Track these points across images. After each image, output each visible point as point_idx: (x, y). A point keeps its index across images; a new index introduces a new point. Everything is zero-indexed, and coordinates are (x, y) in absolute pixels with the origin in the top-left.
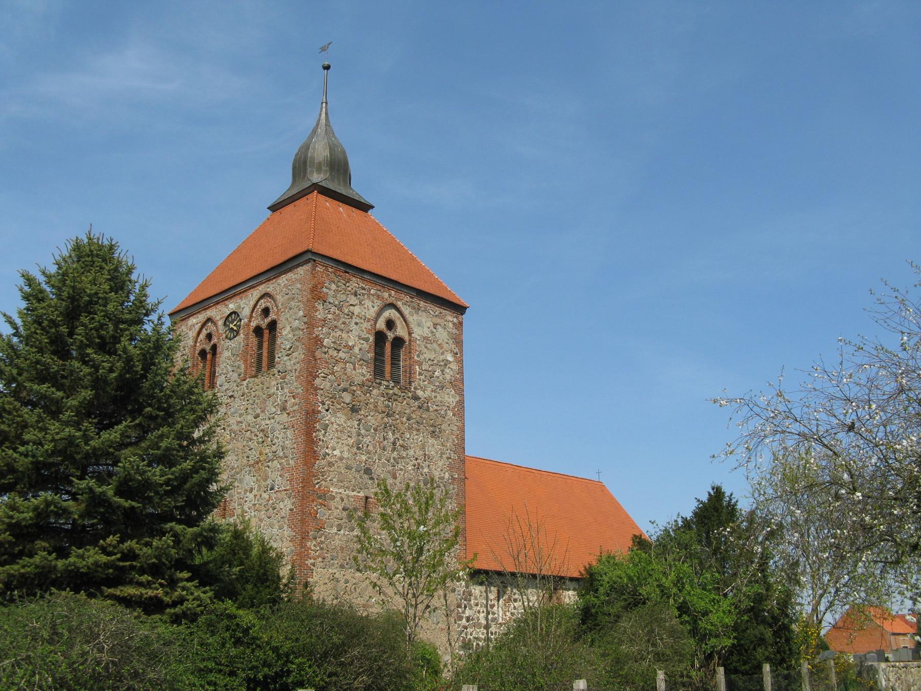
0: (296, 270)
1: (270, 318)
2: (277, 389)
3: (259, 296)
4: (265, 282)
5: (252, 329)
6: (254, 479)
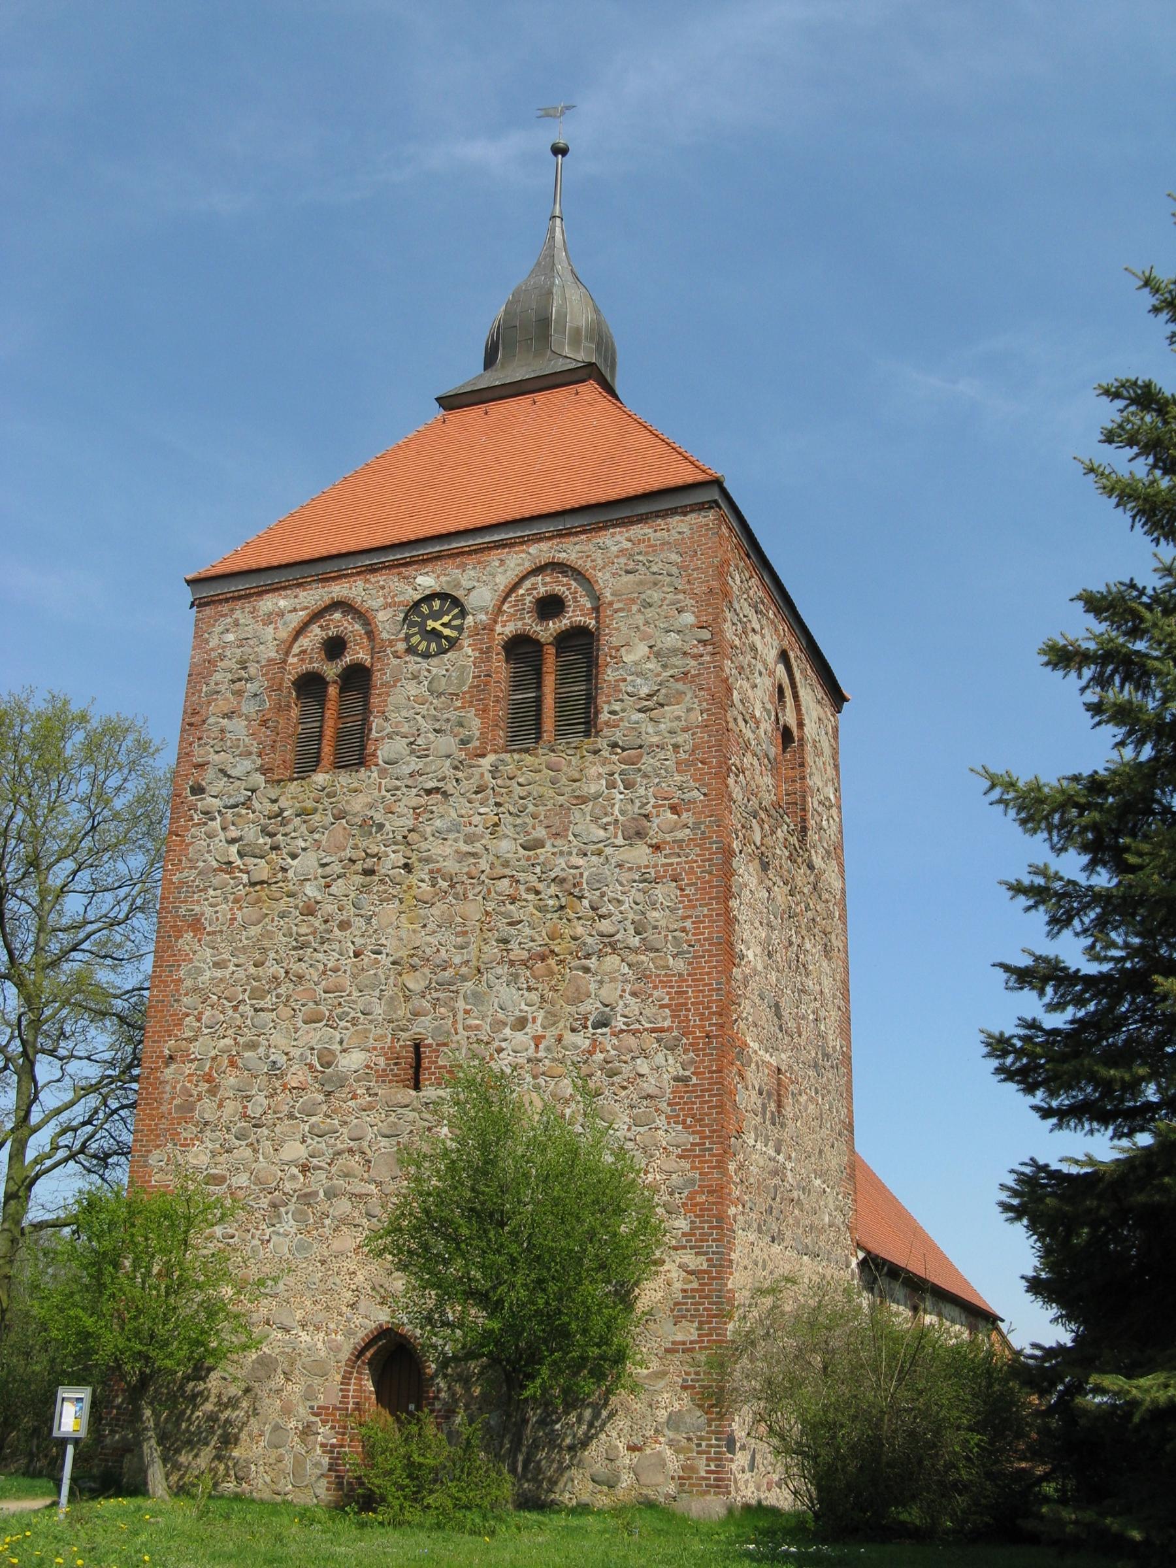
0: (659, 521)
1: (565, 621)
2: (611, 785)
3: (528, 566)
4: (550, 538)
5: (498, 640)
6: (534, 996)
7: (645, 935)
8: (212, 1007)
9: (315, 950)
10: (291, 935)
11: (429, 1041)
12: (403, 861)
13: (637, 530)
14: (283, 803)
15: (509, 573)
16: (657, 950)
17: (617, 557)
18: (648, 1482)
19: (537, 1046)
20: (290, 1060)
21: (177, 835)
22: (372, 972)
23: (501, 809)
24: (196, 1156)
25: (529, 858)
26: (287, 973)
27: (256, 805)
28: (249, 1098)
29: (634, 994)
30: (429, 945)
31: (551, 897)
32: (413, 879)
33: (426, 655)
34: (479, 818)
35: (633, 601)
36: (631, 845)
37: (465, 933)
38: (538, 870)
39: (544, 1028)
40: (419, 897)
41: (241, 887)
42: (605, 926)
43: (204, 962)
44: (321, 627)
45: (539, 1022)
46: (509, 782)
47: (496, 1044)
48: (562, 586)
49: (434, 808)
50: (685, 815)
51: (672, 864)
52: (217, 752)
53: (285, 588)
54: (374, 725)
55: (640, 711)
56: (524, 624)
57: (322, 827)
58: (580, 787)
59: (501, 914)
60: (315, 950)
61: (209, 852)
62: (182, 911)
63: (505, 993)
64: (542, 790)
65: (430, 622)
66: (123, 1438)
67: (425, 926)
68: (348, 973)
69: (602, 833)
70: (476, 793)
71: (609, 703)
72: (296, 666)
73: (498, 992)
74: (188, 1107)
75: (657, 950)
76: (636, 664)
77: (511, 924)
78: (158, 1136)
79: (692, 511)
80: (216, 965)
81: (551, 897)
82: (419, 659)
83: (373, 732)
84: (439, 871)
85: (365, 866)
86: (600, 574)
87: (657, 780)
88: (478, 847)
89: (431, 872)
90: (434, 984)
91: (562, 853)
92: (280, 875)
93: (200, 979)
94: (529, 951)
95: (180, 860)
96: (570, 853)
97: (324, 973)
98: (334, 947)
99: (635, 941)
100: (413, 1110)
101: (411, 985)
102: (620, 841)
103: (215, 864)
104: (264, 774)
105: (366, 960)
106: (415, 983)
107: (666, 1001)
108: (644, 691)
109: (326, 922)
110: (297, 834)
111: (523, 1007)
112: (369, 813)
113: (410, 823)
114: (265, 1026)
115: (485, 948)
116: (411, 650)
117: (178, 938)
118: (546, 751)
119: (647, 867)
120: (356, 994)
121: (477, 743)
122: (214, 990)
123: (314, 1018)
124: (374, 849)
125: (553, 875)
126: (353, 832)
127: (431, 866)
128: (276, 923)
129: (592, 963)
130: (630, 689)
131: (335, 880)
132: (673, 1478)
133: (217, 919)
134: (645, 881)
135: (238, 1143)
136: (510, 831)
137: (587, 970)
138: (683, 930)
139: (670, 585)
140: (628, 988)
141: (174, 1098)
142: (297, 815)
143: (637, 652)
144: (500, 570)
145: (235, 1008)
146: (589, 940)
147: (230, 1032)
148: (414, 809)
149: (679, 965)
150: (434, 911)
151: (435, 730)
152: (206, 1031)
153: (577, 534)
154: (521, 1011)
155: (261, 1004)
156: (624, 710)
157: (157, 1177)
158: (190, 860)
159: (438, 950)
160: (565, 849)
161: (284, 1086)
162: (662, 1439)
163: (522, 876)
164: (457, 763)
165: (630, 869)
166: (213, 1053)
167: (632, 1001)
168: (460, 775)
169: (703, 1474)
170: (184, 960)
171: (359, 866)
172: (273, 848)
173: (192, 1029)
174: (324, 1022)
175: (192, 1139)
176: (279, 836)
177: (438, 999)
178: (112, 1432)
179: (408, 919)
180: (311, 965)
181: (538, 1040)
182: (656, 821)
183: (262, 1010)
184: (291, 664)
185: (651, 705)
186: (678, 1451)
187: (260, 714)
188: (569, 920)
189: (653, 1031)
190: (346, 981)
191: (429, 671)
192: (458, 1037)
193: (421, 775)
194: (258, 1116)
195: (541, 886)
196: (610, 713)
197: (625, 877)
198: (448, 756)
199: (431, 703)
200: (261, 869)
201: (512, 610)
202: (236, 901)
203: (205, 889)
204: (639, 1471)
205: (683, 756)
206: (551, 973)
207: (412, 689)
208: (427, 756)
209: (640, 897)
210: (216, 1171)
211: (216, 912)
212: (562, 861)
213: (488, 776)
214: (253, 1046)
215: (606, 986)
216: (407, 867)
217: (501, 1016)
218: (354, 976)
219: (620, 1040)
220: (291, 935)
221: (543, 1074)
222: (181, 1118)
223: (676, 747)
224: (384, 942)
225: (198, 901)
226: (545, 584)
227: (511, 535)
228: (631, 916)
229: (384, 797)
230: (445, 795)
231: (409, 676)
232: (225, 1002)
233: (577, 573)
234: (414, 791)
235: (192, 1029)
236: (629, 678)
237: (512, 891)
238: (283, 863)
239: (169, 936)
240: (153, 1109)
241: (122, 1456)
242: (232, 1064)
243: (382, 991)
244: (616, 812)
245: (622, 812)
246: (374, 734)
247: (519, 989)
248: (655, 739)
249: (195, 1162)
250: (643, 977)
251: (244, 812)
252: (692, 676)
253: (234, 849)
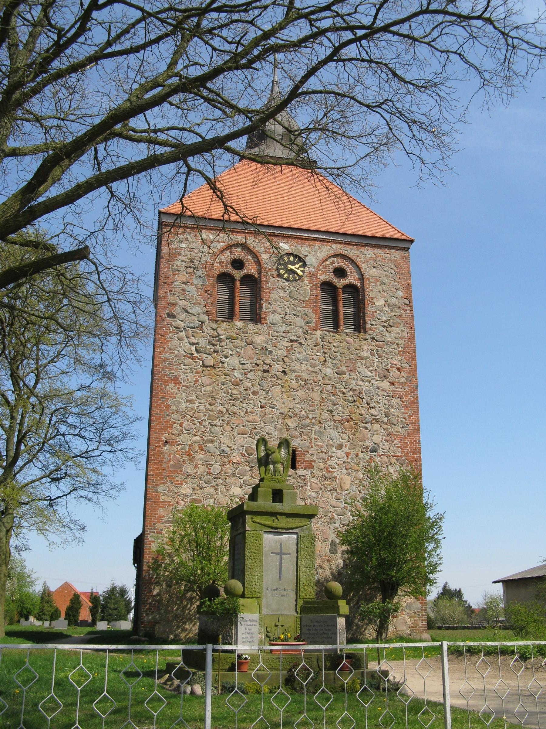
0: (386, 250)
2: (373, 355)
3: (331, 253)
4: (340, 243)
5: (319, 282)
6: (345, 436)
7: (389, 418)
8: (188, 420)
9: (241, 402)
10: (228, 393)
11: (300, 449)
12: (282, 370)
13: (377, 251)
14: (220, 331)
15: (323, 253)
16: (395, 425)
17: (370, 260)
18: (400, 629)
19: (347, 457)
20: (232, 450)
21: (161, 335)
22: (270, 416)
23: (326, 355)
24: (185, 489)
25: (340, 378)
26: (227, 410)
27: (205, 329)
28: (211, 465)
29: (386, 441)
30: (297, 408)
31: (350, 396)
32: (287, 378)
33: (287, 280)
34: (316, 357)
35: (378, 280)
36: (382, 381)
37: (313, 406)
38: (344, 384)
39: (350, 449)
40: (291, 386)
41: (199, 366)
42: (373, 411)
43: (182, 399)
44: (230, 252)
45: (348, 447)
46: (329, 345)
47: (330, 454)
48: (346, 266)
49: (296, 349)
50: (403, 373)
51: (399, 391)
52: (181, 300)
53: (212, 229)
54: (264, 305)
55: (383, 326)
56: (330, 277)
57: (241, 346)
58: (360, 353)
59: (329, 400)
60: (241, 402)
61: (180, 347)
62: (167, 372)
63: (334, 434)
64: (344, 351)
65: (290, 266)
66: (154, 618)
67: (294, 399)
68: (259, 415)
69: (370, 373)
70: (315, 346)
71: (370, 320)
72: (218, 269)
73: (329, 432)
74: (178, 467)
75: (395, 425)
76: (380, 307)
77: (333, 405)
78: (162, 478)
79: (400, 250)
80: (188, 401)
81: (350, 396)
82: (284, 281)
83: (264, 308)
84: (299, 376)
85: (264, 368)
86: (363, 265)
87: (391, 357)
88: (317, 369)
89: (296, 376)
90: (300, 425)
91: (354, 379)
92: (220, 364)
93: (180, 407)
94: (342, 417)
95: (164, 348)
96: (357, 379)
97: (247, 413)
98: (251, 402)
99: (386, 420)
100: (294, 478)
101: (290, 424)
102: (377, 378)
103: (185, 354)
104: (208, 316)
105: (267, 410)
106: (292, 423)
107: (399, 445)
108: (384, 319)
109: (246, 390)
110: (228, 347)
111: (340, 440)
112: (265, 345)
113: (285, 353)
114: (217, 433)
115: (323, 413)
116: (279, 275)
117: (166, 386)
118: (344, 335)
119: (389, 391)
120: (263, 425)
121: (314, 325)
122: (188, 413)
123: (243, 433)
124: (268, 362)
125: (351, 387)
126: (257, 352)
127: (296, 374)
128: (220, 387)
129: (369, 426)
130: (378, 317)
131: (249, 372)
132: (409, 627)
133: (188, 380)
134: (388, 396)
135: (206, 485)
136: (330, 365)
137: (366, 428)
138: (404, 418)
139: (392, 278)
140: (384, 438)
141: (170, 461)
142: (227, 339)
143: (380, 302)
144: (319, 251)
145: (200, 423)
146: (367, 416)
147: (198, 434)
148: (286, 347)
149: (403, 431)
150: (298, 393)
151: (294, 314)
152: (185, 432)
153: (352, 245)
154: (340, 441)
155: (215, 423)
156: (376, 325)
157: (163, 498)
158: (170, 349)
159: (301, 411)
160: (355, 377)
161: (229, 461)
162: (404, 613)
163: (337, 386)
164: (305, 331)
165: (383, 390)
166: (190, 442)
167: (386, 443)
168: (307, 337)
169: (421, 626)
170: (171, 397)
171: (261, 368)
172: (215, 351)
173: (177, 430)
174: (248, 435)
175: (181, 481)
176: (218, 346)
177: (303, 432)
178: (147, 615)
179: (286, 395)
180: (240, 409)
181: (348, 455)
182: (392, 373)
183: (215, 425)
184: (216, 266)
185: (388, 326)
186: (410, 618)
187: (203, 287)
188: (358, 407)
189: (395, 456)
190: (257, 418)
191: (289, 287)
192: (312, 449)
193: (288, 333)
194: (216, 473)
195: (345, 391)
196: (371, 324)
197: (380, 393)
198: (301, 327)
199: (291, 302)
200: (210, 361)
201: (324, 270)
202: (197, 373)
203: (180, 364)
204: (396, 625)
205: (401, 349)
206: (352, 428)
207: (281, 293)
208: (291, 325)
209: (386, 402)
210: (196, 497)
211: (187, 376)
212: (354, 382)
213: (319, 339)
214: (212, 442)
215: (375, 436)
216: (284, 372)
217: (331, 442)
218: (262, 417)
219: (381, 458)
220: (228, 393)
221: (351, 468)
222: (175, 471)
223: (398, 344)
224: (276, 403)
225: (176, 370)
226: (338, 262)
227: (324, 237)
228: (383, 409)
229: (272, 339)
230: (301, 344)
231: (280, 287)
232: (195, 419)
233: (353, 262)
234: (286, 339)
235: (177, 430)
236: (378, 312)
237: (333, 391)
238: (222, 360)
239: (161, 384)
240: (158, 465)
241: (154, 625)
242: (201, 449)
243: (276, 425)
244: (375, 366)
245: (378, 367)
246: (264, 309)
247: (338, 432)
248: (390, 340)
249: (184, 492)
250: (390, 434)
251: (199, 331)
252: (404, 318)
253: (193, 348)
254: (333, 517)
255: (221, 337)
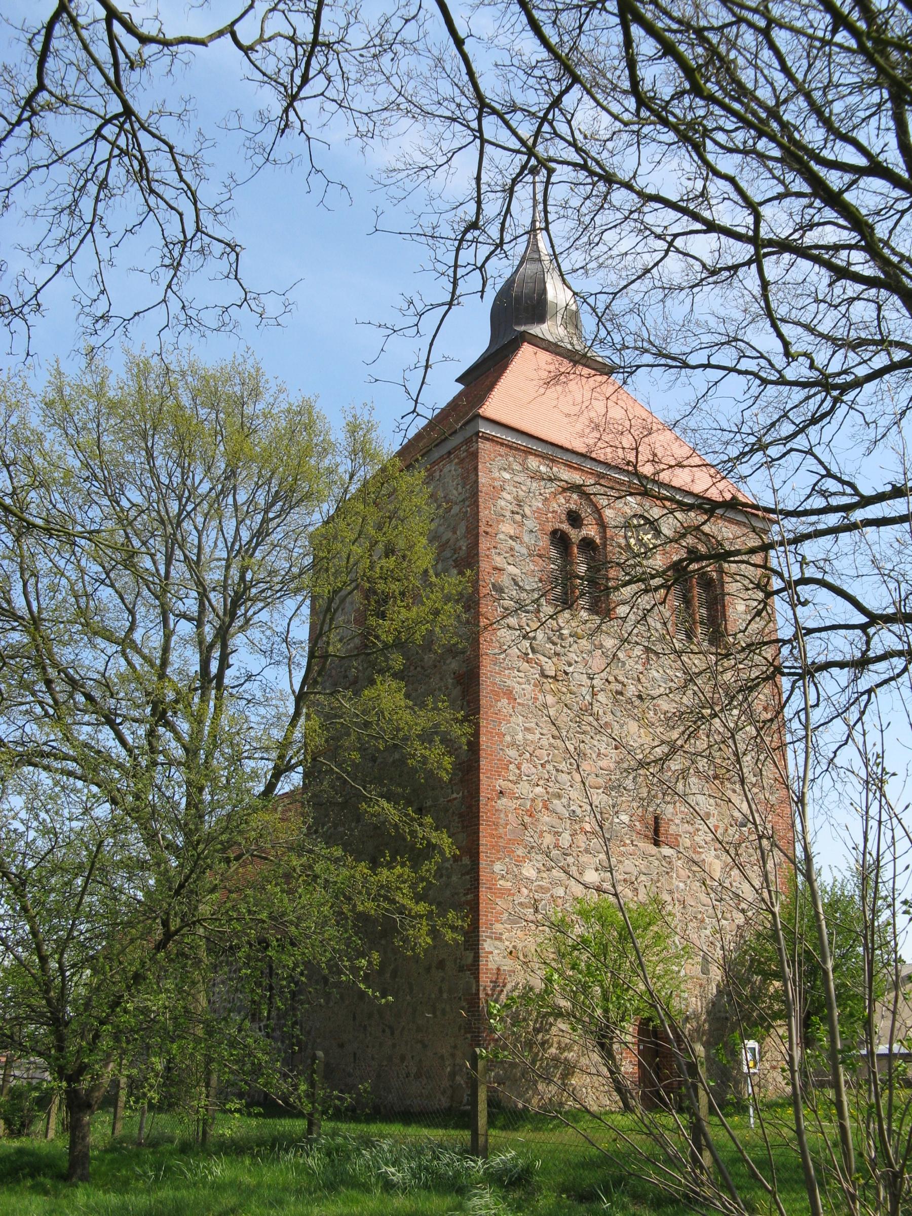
78: (498, 851)
147: (541, 782)
152: (525, 778)
166: (531, 796)
214: (559, 797)
216: (640, 697)
225: (509, 677)
254: (703, 921)
255: (563, 632)
